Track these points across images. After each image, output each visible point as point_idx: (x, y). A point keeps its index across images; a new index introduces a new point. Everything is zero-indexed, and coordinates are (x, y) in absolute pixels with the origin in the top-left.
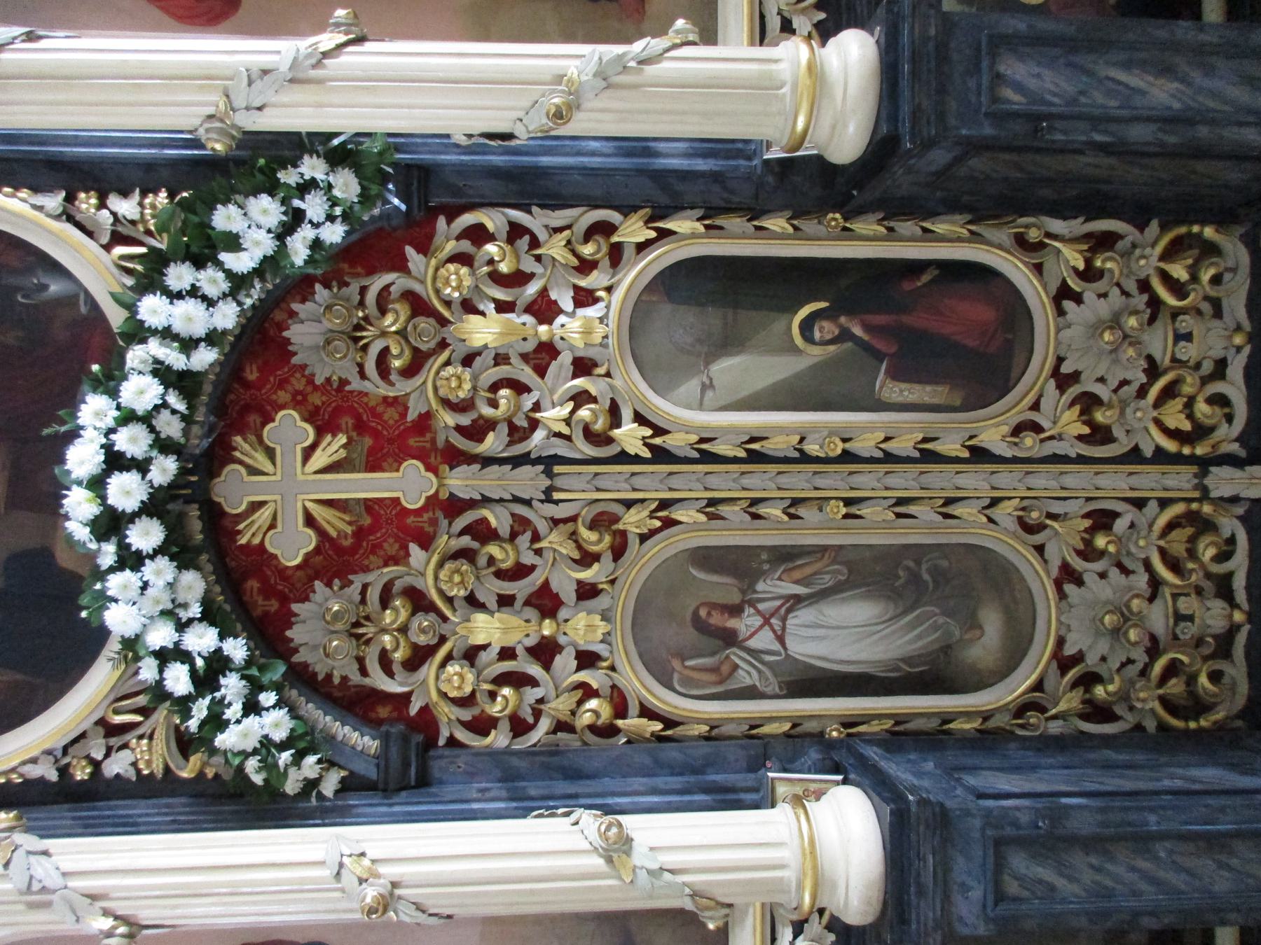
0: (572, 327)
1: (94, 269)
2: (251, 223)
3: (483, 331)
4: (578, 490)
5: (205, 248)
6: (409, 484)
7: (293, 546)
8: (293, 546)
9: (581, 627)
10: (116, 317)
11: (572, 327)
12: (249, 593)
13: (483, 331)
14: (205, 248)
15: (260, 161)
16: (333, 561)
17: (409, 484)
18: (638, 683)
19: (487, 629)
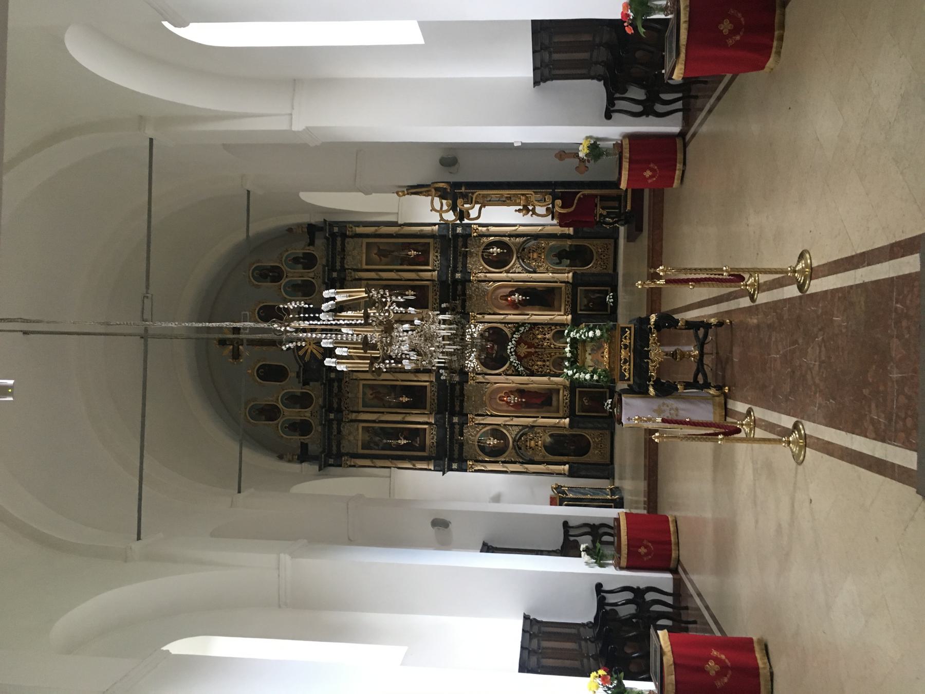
0: (547, 336)
1: (507, 330)
2: (522, 329)
3: (539, 337)
4: (547, 352)
5: (518, 331)
6: (533, 350)
7: (522, 355)
8: (522, 355)
9: (548, 363)
10: (510, 336)
11: (547, 336)
12: (519, 358)
13: (539, 337)
14: (518, 331)
15: (523, 324)
16: (525, 357)
17: (533, 350)
18: (552, 368)
19: (539, 363)
